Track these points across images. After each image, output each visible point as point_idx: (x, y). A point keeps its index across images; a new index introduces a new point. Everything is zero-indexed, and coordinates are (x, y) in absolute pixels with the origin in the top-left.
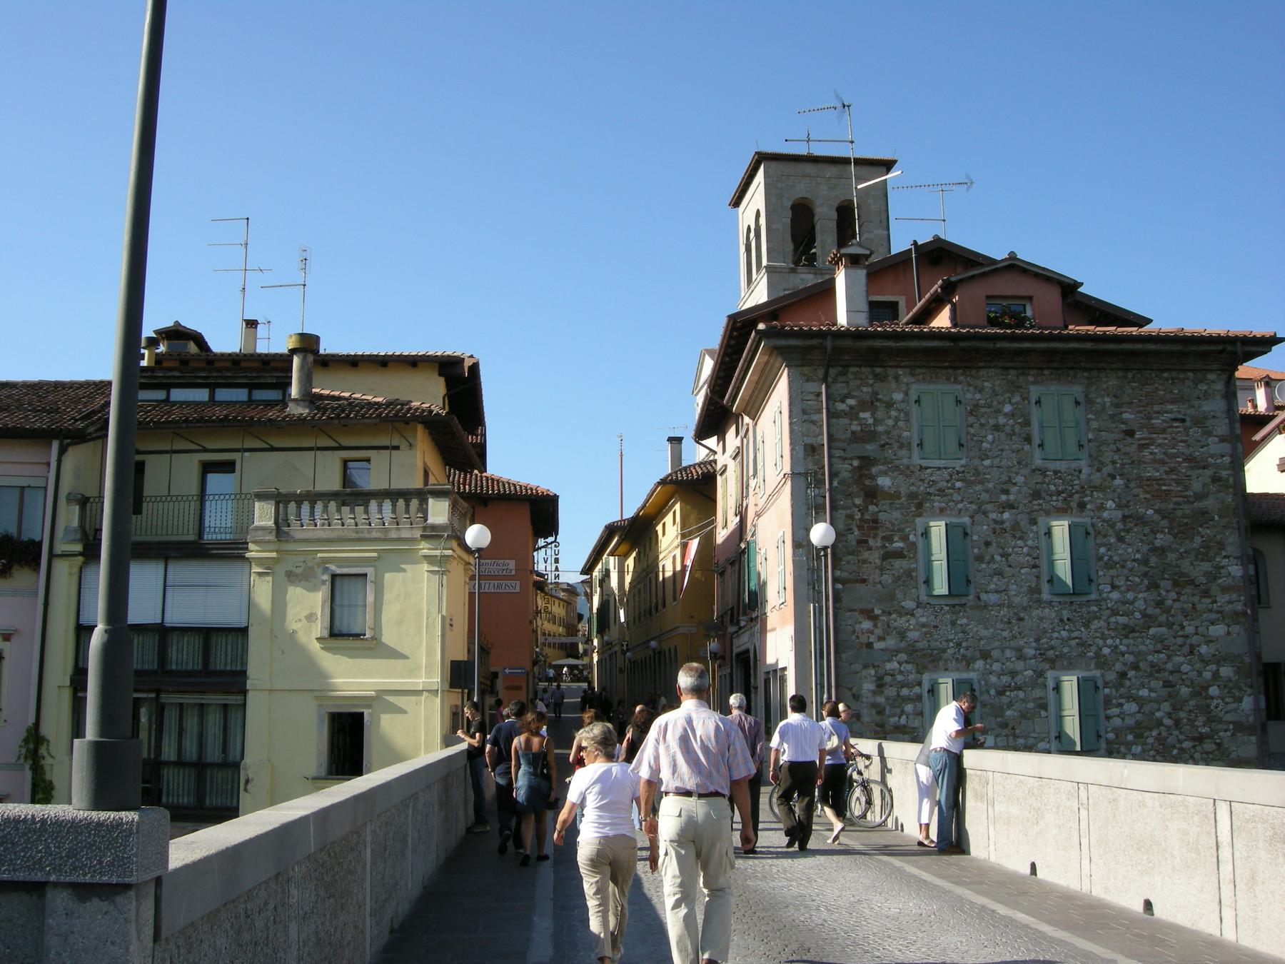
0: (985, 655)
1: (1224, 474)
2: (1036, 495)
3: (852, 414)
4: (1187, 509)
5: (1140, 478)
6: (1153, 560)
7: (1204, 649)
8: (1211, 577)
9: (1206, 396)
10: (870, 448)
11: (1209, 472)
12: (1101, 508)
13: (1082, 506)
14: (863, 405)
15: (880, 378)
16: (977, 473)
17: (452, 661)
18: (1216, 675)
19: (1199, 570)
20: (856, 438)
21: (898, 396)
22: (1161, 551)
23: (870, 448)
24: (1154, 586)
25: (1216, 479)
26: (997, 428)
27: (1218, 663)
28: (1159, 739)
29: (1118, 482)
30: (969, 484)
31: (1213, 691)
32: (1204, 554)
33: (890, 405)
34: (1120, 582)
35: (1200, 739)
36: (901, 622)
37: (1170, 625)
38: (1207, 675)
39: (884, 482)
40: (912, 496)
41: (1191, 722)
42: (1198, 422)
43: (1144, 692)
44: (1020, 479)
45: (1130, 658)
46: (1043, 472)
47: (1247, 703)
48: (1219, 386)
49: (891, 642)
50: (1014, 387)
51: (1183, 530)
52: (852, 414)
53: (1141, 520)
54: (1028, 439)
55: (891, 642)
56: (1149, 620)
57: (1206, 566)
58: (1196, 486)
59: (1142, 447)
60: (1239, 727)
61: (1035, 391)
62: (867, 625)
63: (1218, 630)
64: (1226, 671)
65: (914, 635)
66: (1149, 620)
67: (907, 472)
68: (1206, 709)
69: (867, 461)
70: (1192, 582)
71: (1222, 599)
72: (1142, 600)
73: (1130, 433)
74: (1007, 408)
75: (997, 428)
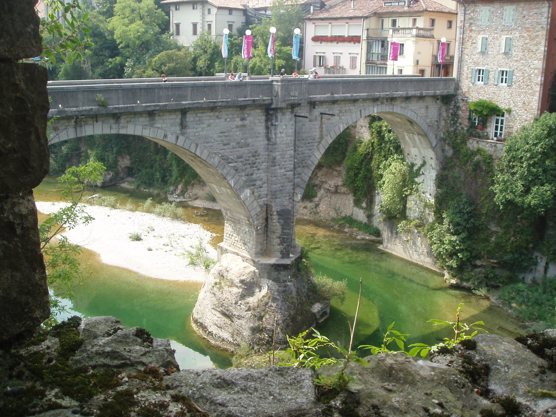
0: (487, 64)
1: (545, 26)
2: (502, 31)
3: (469, 14)
4: (534, 34)
5: (525, 27)
6: (524, 46)
7: (532, 66)
8: (537, 50)
9: (543, 7)
10: (472, 21)
11: (541, 26)
12: (515, 34)
13: (511, 33)
14: (472, 12)
15: (475, 6)
16: (491, 26)
17: (397, 60)
18: (534, 72)
19: (534, 48)
20: (470, 19)
21: (478, 10)
22: (527, 44)
23: (472, 21)
24: (523, 51)
25: (542, 27)
26: (496, 16)
27: (535, 69)
28: (519, 84)
29: (520, 28)
30: (489, 28)
31: (533, 75)
32: (536, 45)
33: (477, 12)
34: (516, 50)
35: (528, 85)
36: (473, 57)
37: (525, 60)
38: (532, 72)
39: (473, 28)
40: (479, 31)
41: (526, 82)
42: (540, 14)
43: (518, 74)
44: (499, 27)
45: (516, 67)
46: (504, 26)
47: (540, 78)
48: (547, 5)
49: (471, 60)
50: (502, 7)
51: (532, 39)
52: (469, 14)
53: (523, 37)
54: (502, 19)
55: (471, 60)
56: (521, 59)
57: (536, 48)
58: (537, 29)
59: (527, 20)
60: (537, 84)
61: (505, 7)
62: (467, 57)
63: (536, 62)
64: (536, 71)
65: (475, 59)
66: (521, 59)
67: (478, 26)
68: (530, 79)
69: (471, 24)
70: (532, 51)
71: (538, 55)
72: (520, 54)
73: (524, 17)
74: (499, 12)
75: (496, 16)
